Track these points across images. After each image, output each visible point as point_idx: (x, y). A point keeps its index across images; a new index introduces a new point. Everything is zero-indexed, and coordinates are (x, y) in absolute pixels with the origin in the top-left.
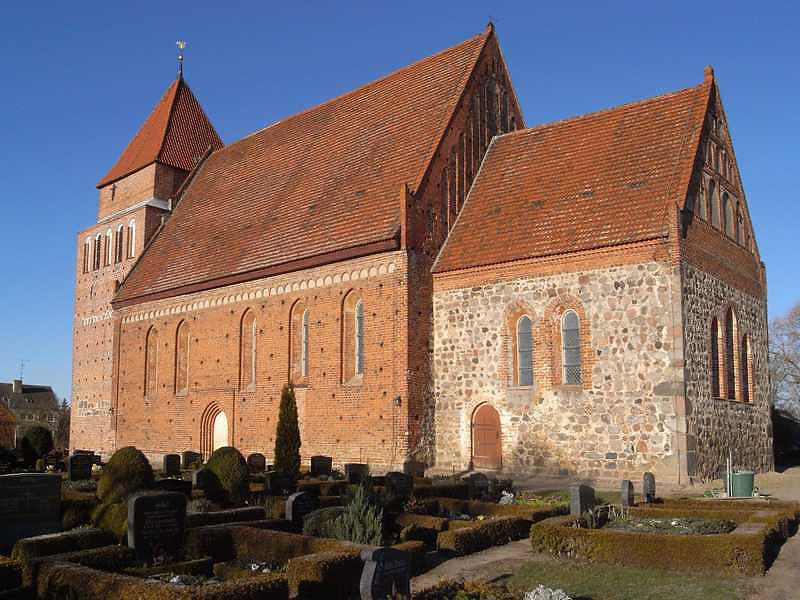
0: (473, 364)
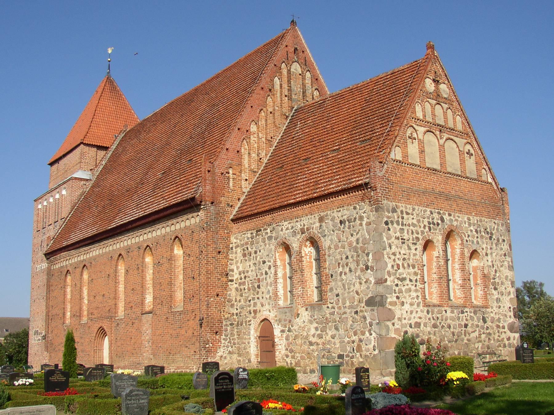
0: (257, 289)
